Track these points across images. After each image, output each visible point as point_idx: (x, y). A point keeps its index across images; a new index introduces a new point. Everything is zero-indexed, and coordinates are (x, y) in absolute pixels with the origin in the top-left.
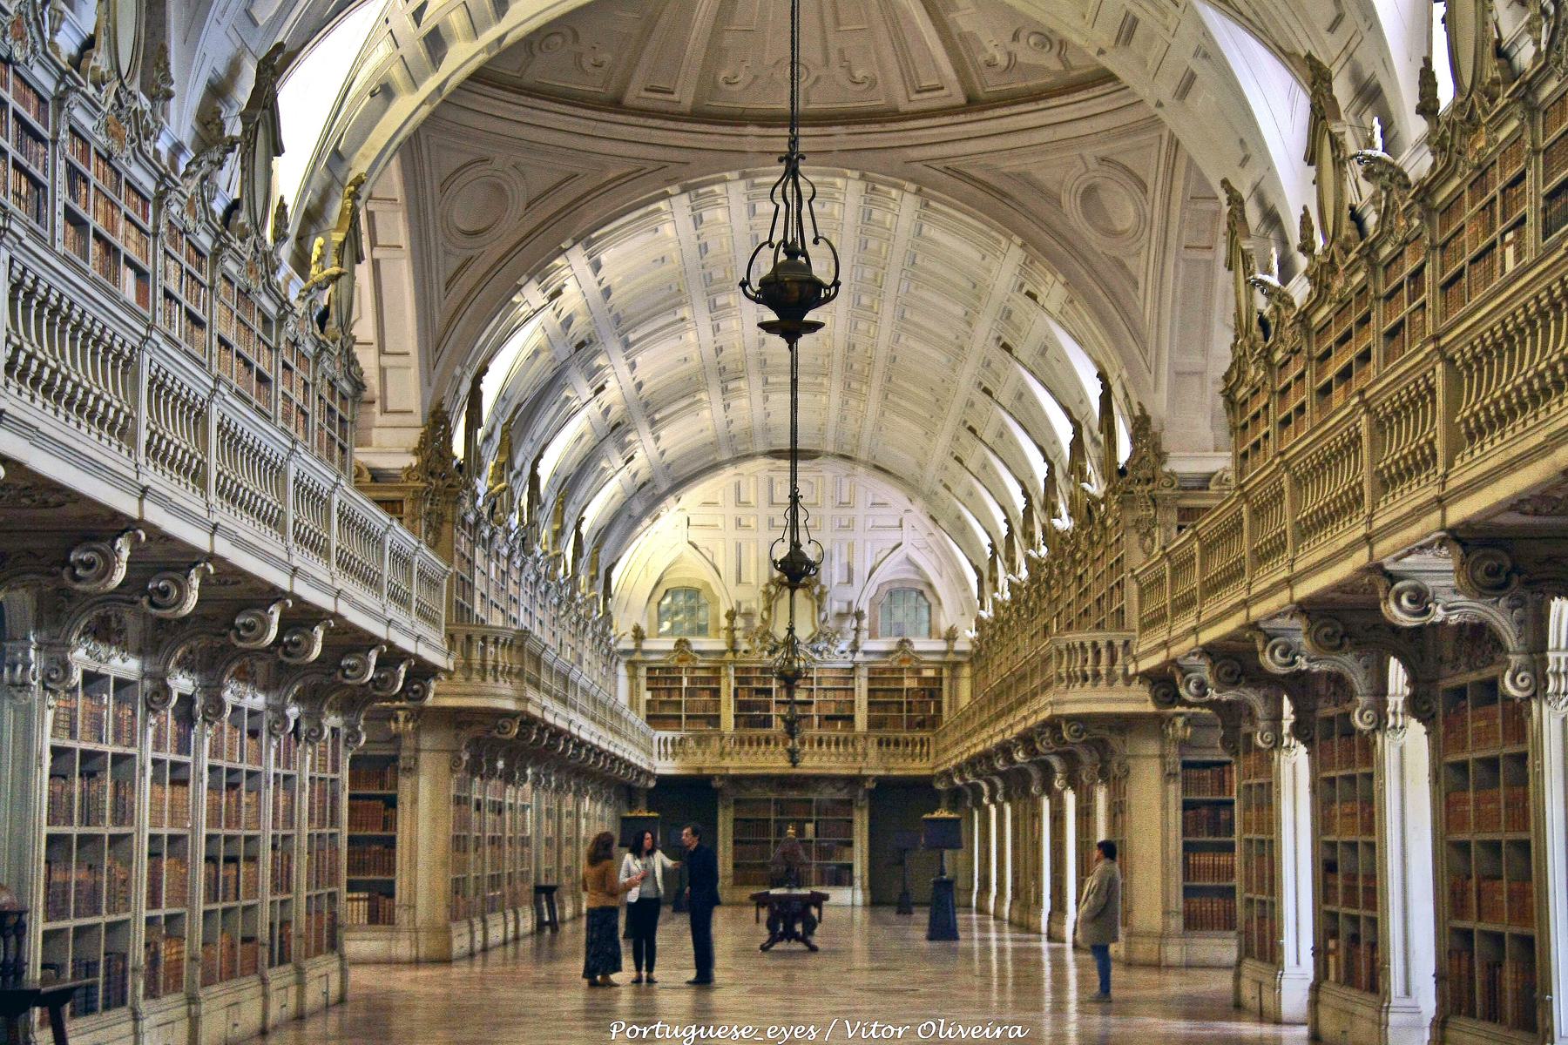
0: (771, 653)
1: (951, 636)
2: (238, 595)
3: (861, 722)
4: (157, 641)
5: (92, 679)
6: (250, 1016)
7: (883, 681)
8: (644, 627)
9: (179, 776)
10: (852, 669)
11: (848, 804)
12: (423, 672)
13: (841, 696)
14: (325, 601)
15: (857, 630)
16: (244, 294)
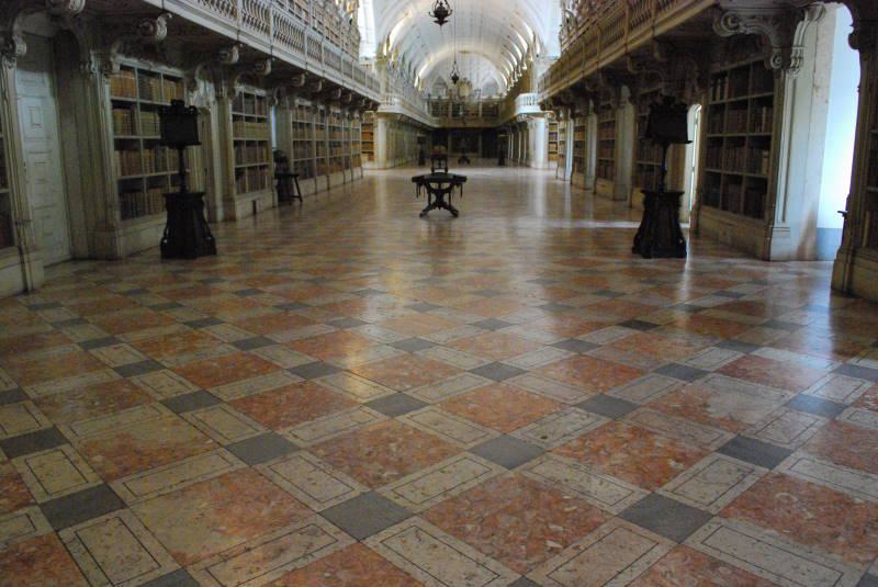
1: (501, 95)
2: (331, 87)
3: (481, 113)
4: (314, 97)
5: (300, 107)
6: (341, 180)
7: (486, 106)
9: (322, 128)
12: (376, 105)
14: (351, 88)
16: (331, 17)
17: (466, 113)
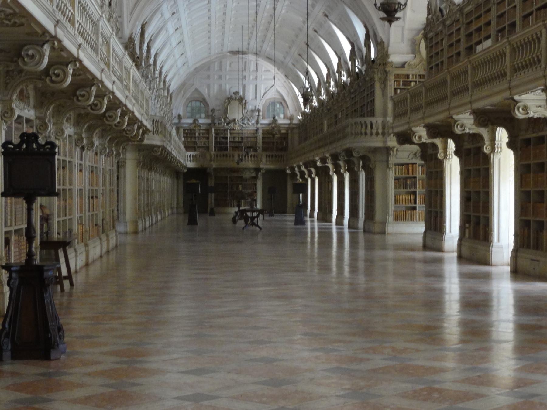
0: (227, 124)
8: (181, 114)
10: (257, 130)
11: (256, 178)
13: (253, 140)
15: (258, 116)
17: (237, 146)
